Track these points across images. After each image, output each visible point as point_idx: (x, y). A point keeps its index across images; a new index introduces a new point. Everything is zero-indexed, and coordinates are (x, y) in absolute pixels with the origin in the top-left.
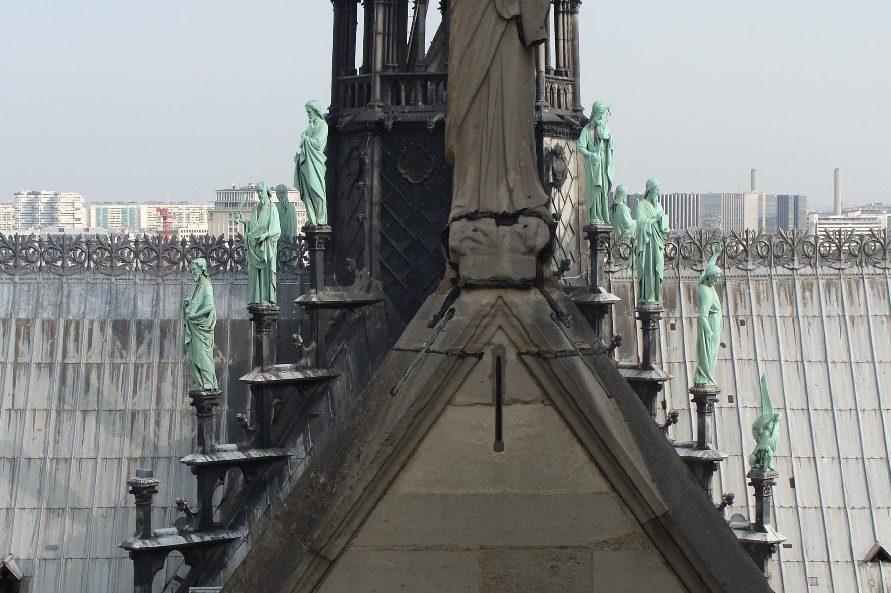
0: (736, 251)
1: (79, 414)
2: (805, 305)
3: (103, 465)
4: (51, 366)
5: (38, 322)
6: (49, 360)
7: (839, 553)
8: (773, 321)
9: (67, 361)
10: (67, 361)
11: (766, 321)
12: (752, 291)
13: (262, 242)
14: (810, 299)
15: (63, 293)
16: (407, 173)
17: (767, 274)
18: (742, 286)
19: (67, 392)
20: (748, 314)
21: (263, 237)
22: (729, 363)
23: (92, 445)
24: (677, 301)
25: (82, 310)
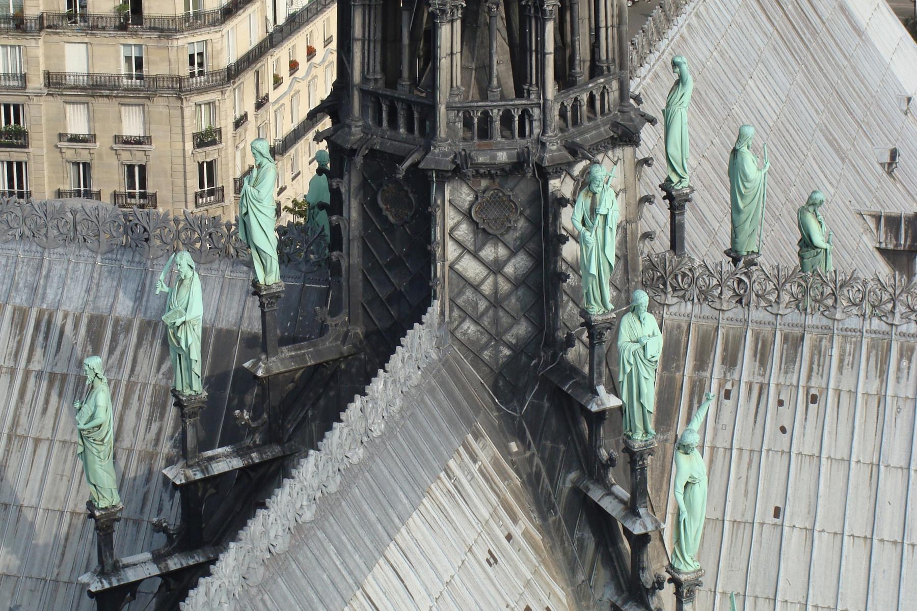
0: (822, 293)
1: (30, 444)
2: (898, 379)
3: (43, 516)
4: (12, 372)
5: (9, 308)
6: (12, 364)
8: (853, 399)
9: (31, 367)
10: (31, 367)
11: (845, 397)
12: (835, 352)
13: (178, 327)
14: (906, 371)
15: (41, 273)
16: (387, 209)
17: (858, 327)
18: (824, 342)
19: (24, 410)
20: (824, 386)
21: (179, 322)
22: (785, 457)
23: (36, 489)
24: (740, 355)
25: (58, 298)
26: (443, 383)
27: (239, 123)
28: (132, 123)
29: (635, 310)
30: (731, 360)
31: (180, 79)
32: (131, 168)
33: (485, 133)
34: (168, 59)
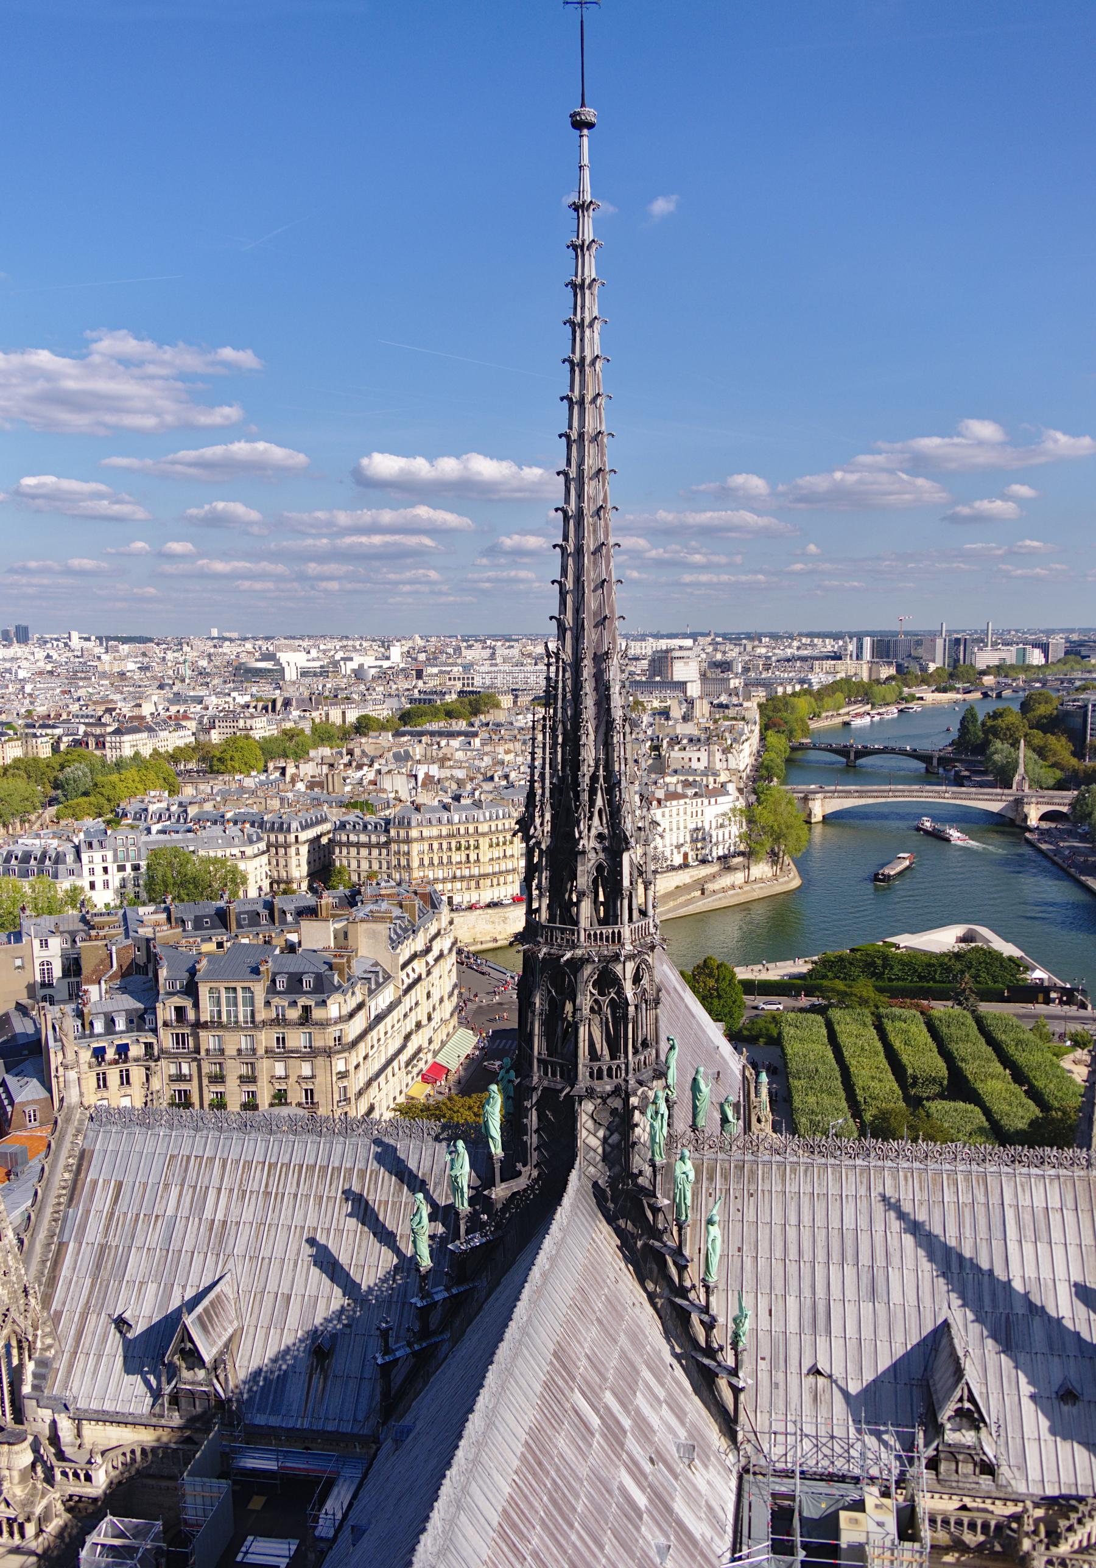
7: (793, 1367)
11: (766, 1193)
26: (584, 1197)
27: (357, 1067)
28: (306, 1069)
29: (682, 1159)
30: (711, 1179)
31: (330, 1048)
32: (306, 1090)
33: (600, 1077)
34: (325, 1039)
